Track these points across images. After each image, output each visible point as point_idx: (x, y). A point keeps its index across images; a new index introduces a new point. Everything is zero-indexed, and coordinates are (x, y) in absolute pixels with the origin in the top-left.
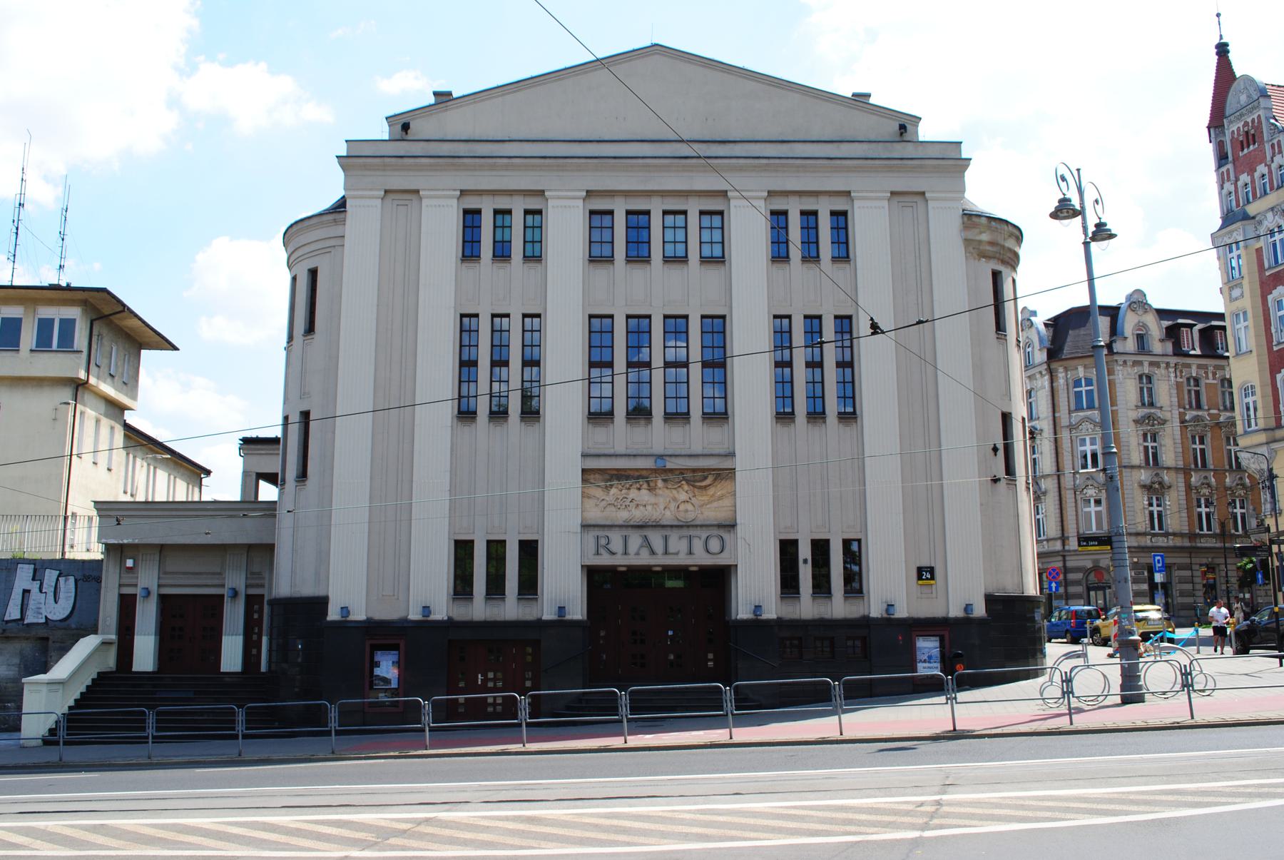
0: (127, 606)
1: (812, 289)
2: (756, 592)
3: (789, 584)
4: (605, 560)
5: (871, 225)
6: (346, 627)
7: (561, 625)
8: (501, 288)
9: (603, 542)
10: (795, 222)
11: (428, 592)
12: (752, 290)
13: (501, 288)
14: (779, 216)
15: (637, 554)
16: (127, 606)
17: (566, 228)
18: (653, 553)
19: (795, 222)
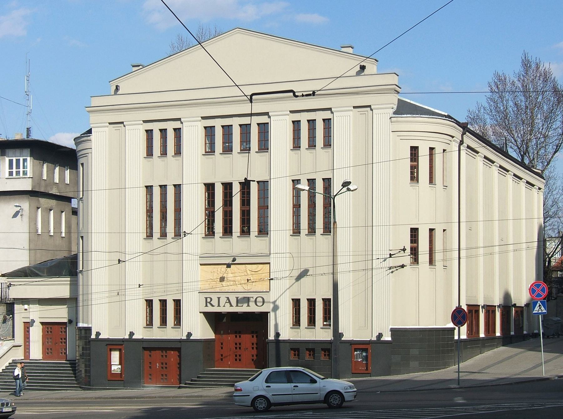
0: (28, 325)
1: (314, 164)
2: (281, 326)
3: (297, 322)
4: (210, 309)
5: (344, 125)
6: (98, 340)
7: (188, 340)
8: (164, 171)
9: (209, 300)
10: (304, 128)
11: (134, 324)
12: (281, 167)
13: (164, 171)
14: (296, 124)
15: (224, 306)
16: (28, 325)
17: (194, 137)
18: (231, 306)
19: (304, 128)
